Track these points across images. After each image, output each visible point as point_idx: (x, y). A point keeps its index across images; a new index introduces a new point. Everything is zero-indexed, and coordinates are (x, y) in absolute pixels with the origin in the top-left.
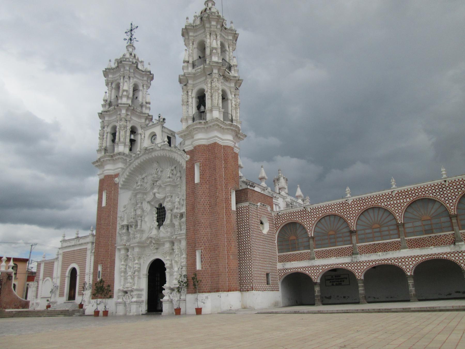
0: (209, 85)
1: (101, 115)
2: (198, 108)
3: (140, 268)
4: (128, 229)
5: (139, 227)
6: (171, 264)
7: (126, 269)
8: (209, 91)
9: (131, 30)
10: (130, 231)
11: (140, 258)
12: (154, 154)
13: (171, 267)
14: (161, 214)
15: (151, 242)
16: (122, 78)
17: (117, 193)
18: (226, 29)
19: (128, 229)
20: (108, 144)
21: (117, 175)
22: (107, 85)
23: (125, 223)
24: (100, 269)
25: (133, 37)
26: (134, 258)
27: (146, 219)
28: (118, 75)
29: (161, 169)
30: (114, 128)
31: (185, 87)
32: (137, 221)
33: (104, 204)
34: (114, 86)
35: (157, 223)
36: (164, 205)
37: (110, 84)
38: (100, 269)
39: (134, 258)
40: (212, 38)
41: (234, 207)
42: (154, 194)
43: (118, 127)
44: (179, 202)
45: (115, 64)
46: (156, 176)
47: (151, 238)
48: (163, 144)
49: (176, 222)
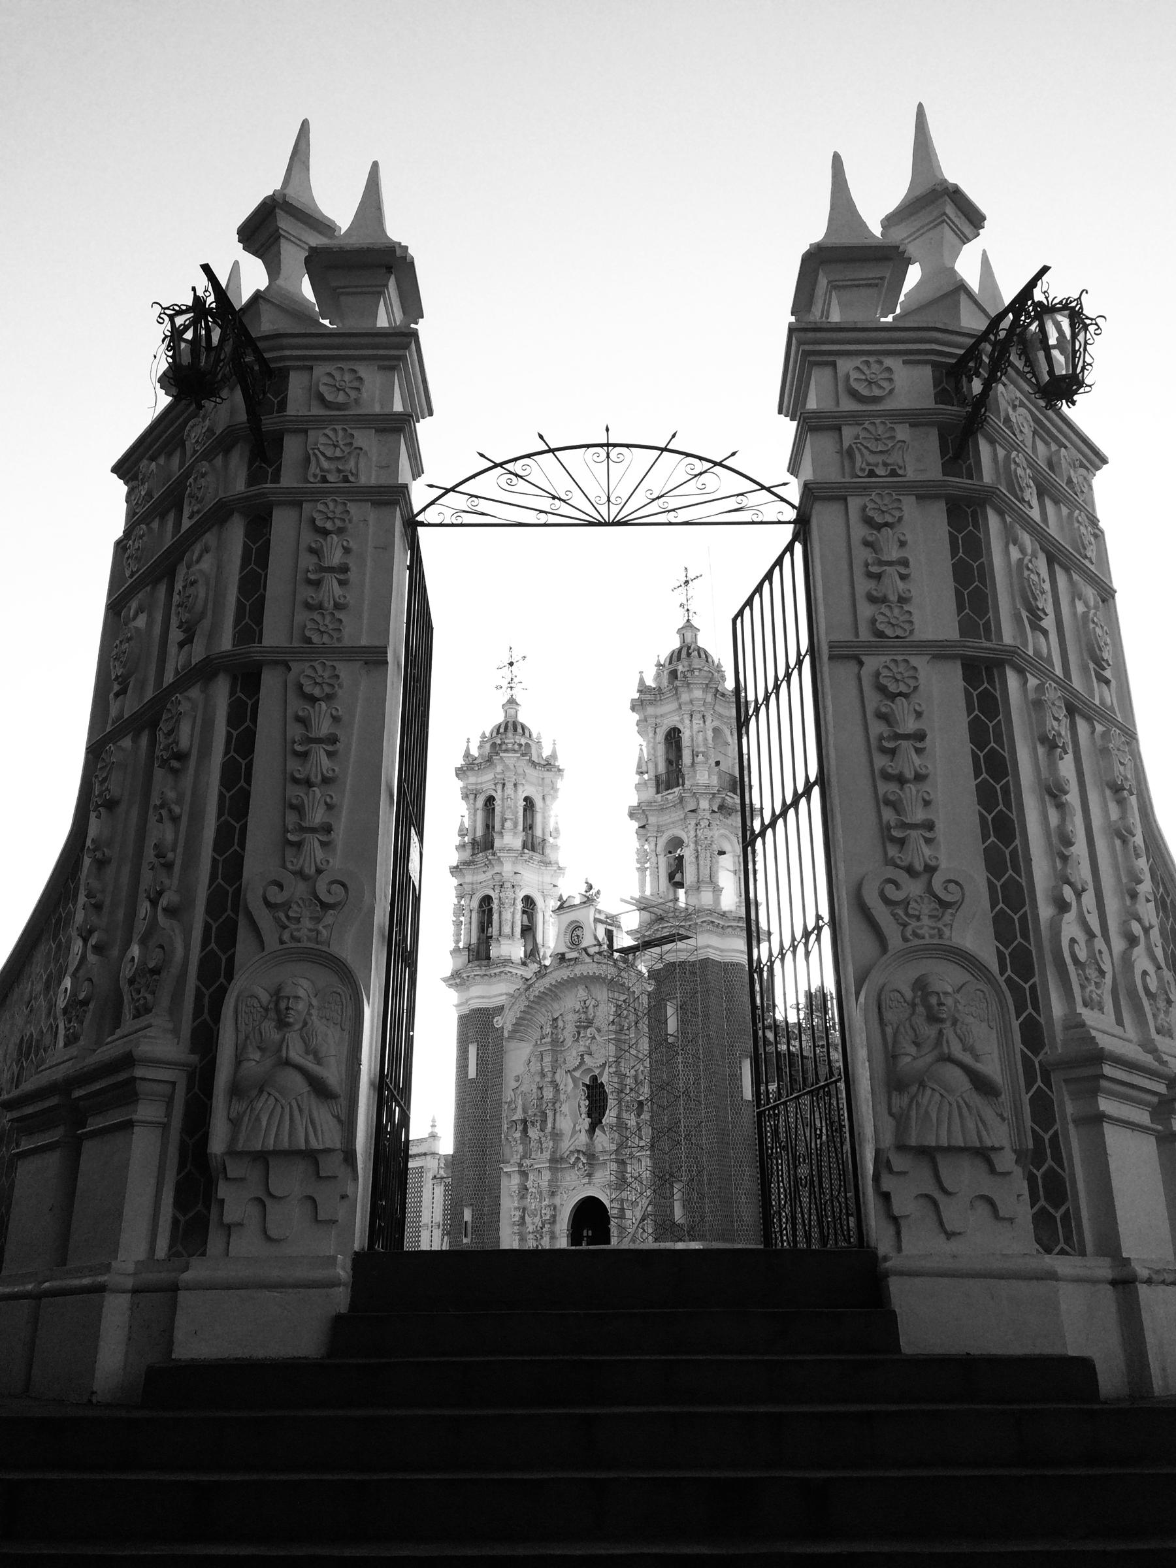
0: (692, 834)
1: (455, 870)
2: (671, 877)
3: (554, 1216)
4: (525, 1131)
5: (549, 1125)
6: (622, 1210)
7: (523, 1218)
8: (692, 846)
9: (511, 664)
10: (530, 1133)
11: (553, 1194)
12: (579, 970)
13: (622, 1216)
14: (596, 1097)
15: (578, 1159)
16: (499, 787)
17: (500, 1052)
18: (723, 695)
19: (525, 1131)
20: (474, 940)
21: (500, 1010)
22: (465, 797)
23: (519, 1115)
24: (467, 1215)
25: (515, 680)
26: (541, 1193)
27: (565, 1108)
28: (490, 776)
29: (593, 1002)
30: (487, 900)
31: (642, 831)
32: (544, 1114)
33: (472, 1073)
34: (480, 802)
35: (588, 1120)
36: (604, 1079)
37: (472, 797)
38: (467, 1215)
39: (541, 1193)
40: (696, 727)
41: (748, 1093)
42: (582, 1056)
43: (496, 901)
44: (636, 1077)
45: (480, 747)
46: (583, 1016)
47: (578, 1151)
48: (597, 949)
49: (632, 1121)
